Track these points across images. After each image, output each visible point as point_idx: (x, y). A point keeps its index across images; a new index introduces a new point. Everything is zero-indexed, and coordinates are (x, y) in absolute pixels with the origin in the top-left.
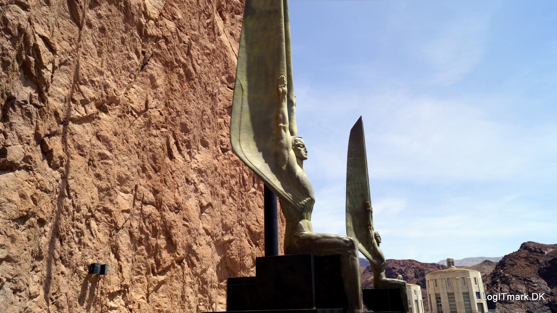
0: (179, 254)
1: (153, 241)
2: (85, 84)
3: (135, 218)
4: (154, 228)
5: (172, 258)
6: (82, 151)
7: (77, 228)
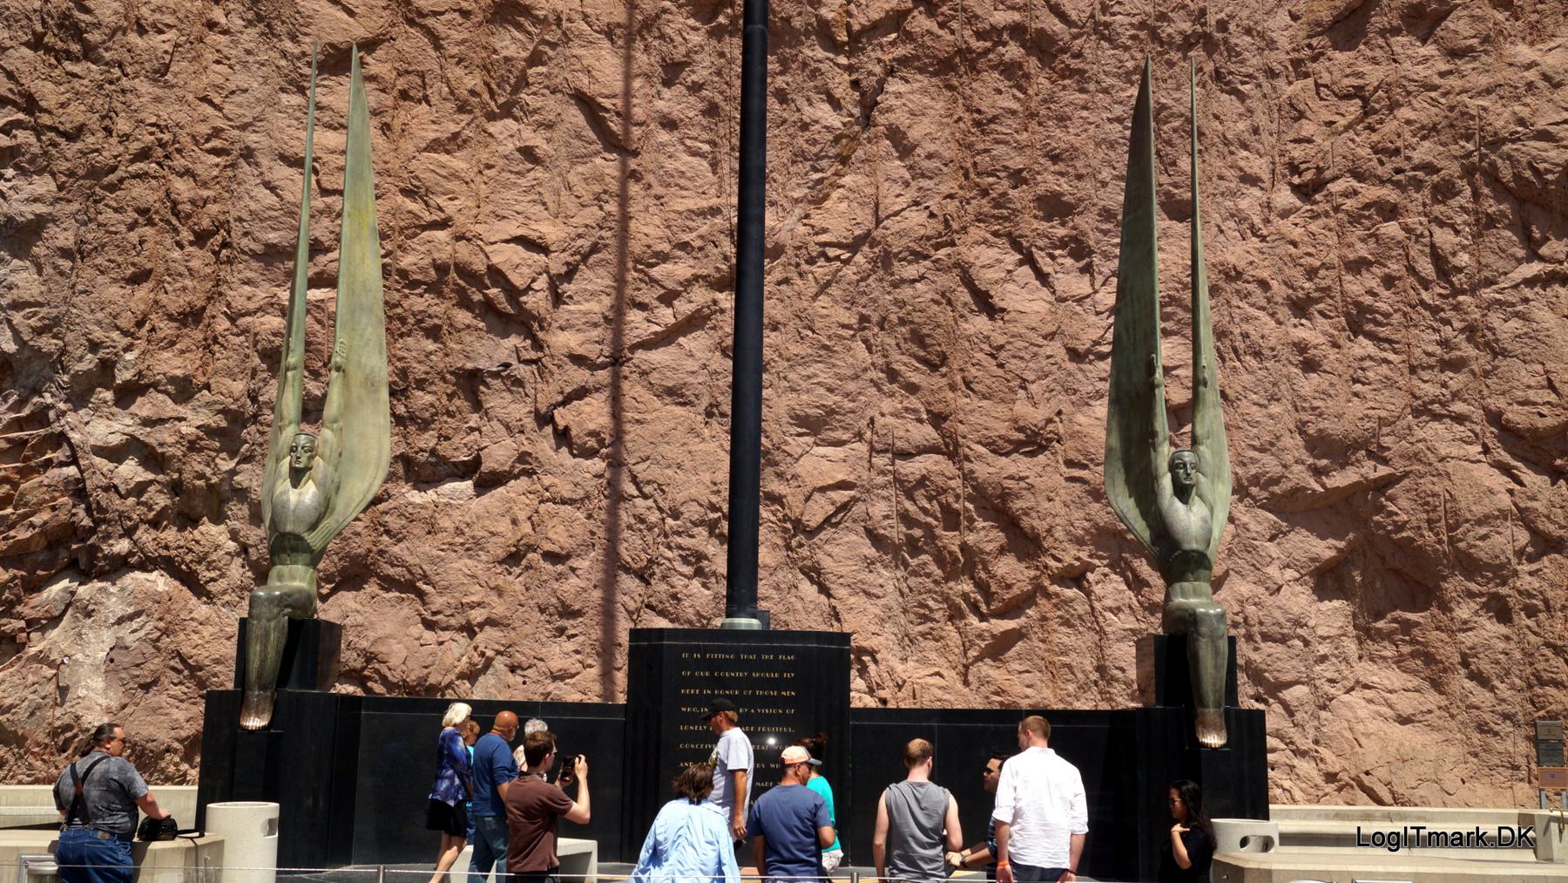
0: (1059, 560)
1: (951, 540)
2: (664, 258)
3: (877, 495)
4: (946, 509)
5: (1033, 573)
6: (682, 396)
7: (680, 547)
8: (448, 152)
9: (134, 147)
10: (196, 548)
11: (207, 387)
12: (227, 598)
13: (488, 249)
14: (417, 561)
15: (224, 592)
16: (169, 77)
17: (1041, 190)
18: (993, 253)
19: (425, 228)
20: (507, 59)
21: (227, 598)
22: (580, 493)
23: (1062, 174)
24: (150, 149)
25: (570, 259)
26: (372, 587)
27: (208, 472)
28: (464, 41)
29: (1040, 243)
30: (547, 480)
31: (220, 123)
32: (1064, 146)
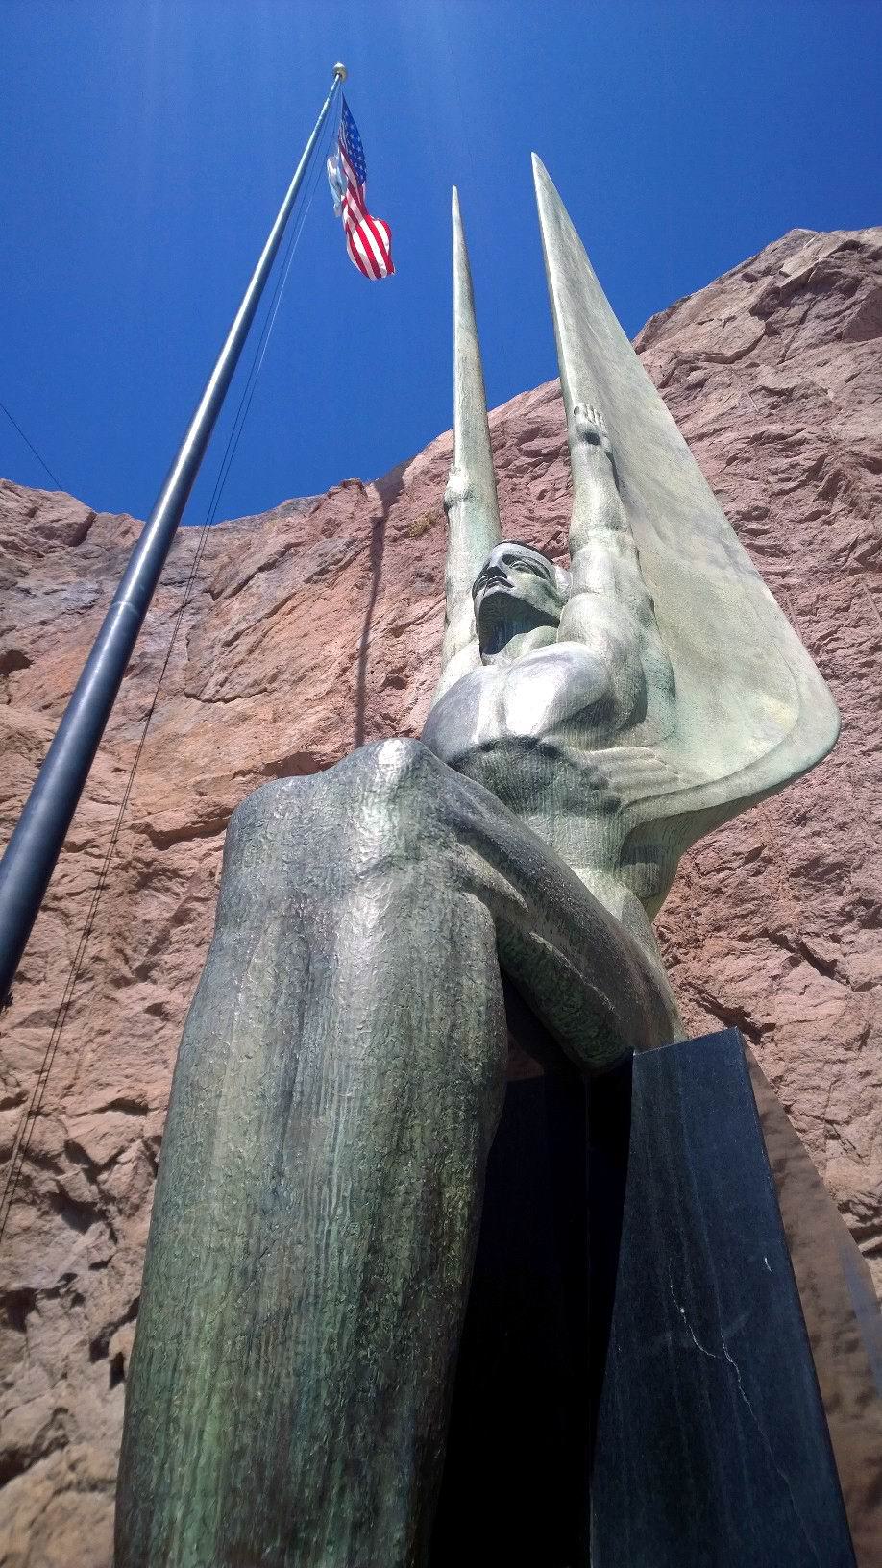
17: (794, 862)
18: (748, 961)
20: (146, 922)
23: (817, 834)
29: (812, 928)
32: (808, 802)
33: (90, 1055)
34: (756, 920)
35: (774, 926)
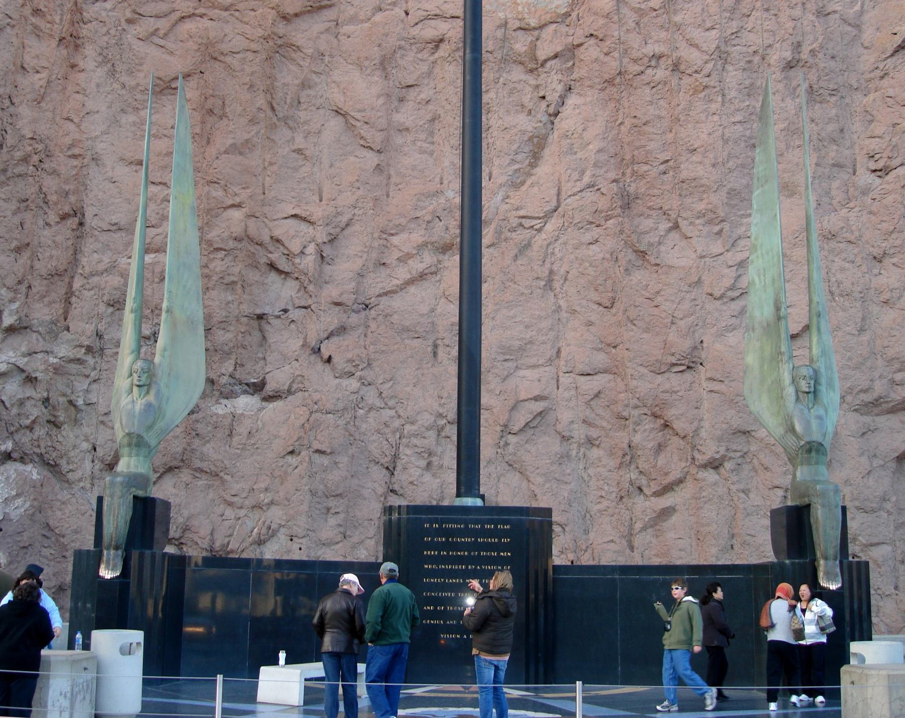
6: (416, 332)
8: (241, 154)
9: (18, 154)
10: (58, 447)
11: (68, 329)
12: (82, 484)
13: (271, 224)
14: (220, 457)
15: (80, 480)
16: (43, 104)
19: (225, 208)
21: (82, 484)
22: (341, 405)
24: (30, 156)
25: (332, 231)
26: (185, 475)
27: (69, 392)
28: (253, 73)
30: (316, 396)
31: (77, 136)
33: (268, 179)
34: (658, 201)
35: (666, 208)
